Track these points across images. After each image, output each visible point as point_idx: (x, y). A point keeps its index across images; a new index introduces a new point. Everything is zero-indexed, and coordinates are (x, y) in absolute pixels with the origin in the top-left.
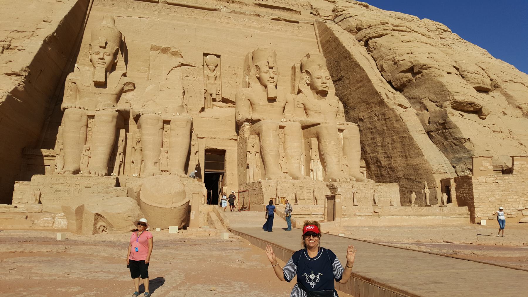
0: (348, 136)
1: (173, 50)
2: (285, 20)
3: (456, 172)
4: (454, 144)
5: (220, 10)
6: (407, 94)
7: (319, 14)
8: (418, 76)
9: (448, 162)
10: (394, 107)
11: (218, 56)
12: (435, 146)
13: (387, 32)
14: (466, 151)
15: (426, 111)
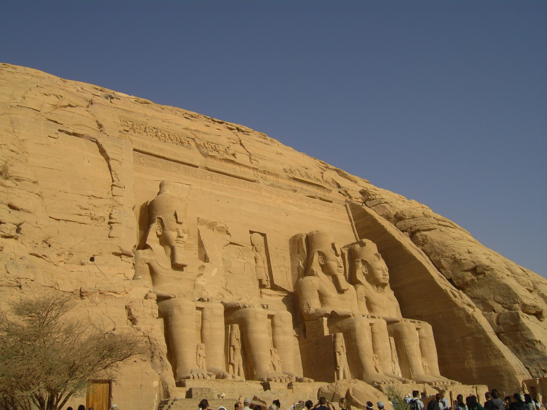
0: (425, 335)
1: (220, 225)
2: (321, 199)
3: (530, 373)
4: (527, 345)
5: (259, 183)
6: (470, 294)
7: (348, 194)
8: (481, 276)
9: (521, 363)
10: (464, 307)
11: (264, 235)
12: (506, 347)
13: (436, 226)
14: (538, 352)
15: (493, 312)
